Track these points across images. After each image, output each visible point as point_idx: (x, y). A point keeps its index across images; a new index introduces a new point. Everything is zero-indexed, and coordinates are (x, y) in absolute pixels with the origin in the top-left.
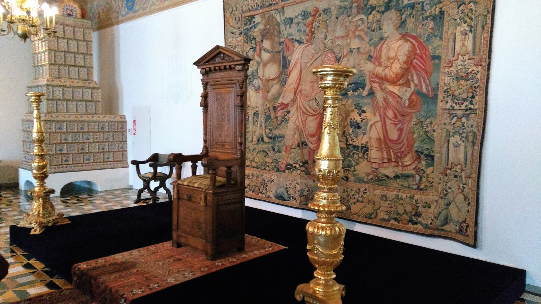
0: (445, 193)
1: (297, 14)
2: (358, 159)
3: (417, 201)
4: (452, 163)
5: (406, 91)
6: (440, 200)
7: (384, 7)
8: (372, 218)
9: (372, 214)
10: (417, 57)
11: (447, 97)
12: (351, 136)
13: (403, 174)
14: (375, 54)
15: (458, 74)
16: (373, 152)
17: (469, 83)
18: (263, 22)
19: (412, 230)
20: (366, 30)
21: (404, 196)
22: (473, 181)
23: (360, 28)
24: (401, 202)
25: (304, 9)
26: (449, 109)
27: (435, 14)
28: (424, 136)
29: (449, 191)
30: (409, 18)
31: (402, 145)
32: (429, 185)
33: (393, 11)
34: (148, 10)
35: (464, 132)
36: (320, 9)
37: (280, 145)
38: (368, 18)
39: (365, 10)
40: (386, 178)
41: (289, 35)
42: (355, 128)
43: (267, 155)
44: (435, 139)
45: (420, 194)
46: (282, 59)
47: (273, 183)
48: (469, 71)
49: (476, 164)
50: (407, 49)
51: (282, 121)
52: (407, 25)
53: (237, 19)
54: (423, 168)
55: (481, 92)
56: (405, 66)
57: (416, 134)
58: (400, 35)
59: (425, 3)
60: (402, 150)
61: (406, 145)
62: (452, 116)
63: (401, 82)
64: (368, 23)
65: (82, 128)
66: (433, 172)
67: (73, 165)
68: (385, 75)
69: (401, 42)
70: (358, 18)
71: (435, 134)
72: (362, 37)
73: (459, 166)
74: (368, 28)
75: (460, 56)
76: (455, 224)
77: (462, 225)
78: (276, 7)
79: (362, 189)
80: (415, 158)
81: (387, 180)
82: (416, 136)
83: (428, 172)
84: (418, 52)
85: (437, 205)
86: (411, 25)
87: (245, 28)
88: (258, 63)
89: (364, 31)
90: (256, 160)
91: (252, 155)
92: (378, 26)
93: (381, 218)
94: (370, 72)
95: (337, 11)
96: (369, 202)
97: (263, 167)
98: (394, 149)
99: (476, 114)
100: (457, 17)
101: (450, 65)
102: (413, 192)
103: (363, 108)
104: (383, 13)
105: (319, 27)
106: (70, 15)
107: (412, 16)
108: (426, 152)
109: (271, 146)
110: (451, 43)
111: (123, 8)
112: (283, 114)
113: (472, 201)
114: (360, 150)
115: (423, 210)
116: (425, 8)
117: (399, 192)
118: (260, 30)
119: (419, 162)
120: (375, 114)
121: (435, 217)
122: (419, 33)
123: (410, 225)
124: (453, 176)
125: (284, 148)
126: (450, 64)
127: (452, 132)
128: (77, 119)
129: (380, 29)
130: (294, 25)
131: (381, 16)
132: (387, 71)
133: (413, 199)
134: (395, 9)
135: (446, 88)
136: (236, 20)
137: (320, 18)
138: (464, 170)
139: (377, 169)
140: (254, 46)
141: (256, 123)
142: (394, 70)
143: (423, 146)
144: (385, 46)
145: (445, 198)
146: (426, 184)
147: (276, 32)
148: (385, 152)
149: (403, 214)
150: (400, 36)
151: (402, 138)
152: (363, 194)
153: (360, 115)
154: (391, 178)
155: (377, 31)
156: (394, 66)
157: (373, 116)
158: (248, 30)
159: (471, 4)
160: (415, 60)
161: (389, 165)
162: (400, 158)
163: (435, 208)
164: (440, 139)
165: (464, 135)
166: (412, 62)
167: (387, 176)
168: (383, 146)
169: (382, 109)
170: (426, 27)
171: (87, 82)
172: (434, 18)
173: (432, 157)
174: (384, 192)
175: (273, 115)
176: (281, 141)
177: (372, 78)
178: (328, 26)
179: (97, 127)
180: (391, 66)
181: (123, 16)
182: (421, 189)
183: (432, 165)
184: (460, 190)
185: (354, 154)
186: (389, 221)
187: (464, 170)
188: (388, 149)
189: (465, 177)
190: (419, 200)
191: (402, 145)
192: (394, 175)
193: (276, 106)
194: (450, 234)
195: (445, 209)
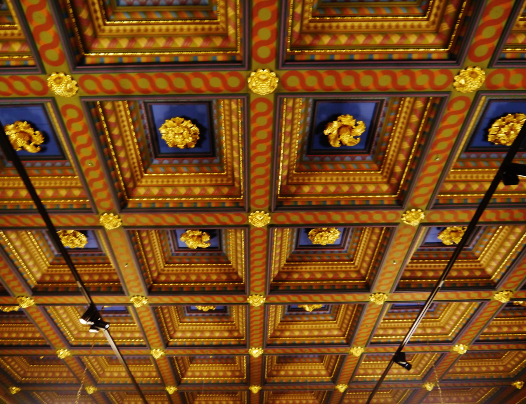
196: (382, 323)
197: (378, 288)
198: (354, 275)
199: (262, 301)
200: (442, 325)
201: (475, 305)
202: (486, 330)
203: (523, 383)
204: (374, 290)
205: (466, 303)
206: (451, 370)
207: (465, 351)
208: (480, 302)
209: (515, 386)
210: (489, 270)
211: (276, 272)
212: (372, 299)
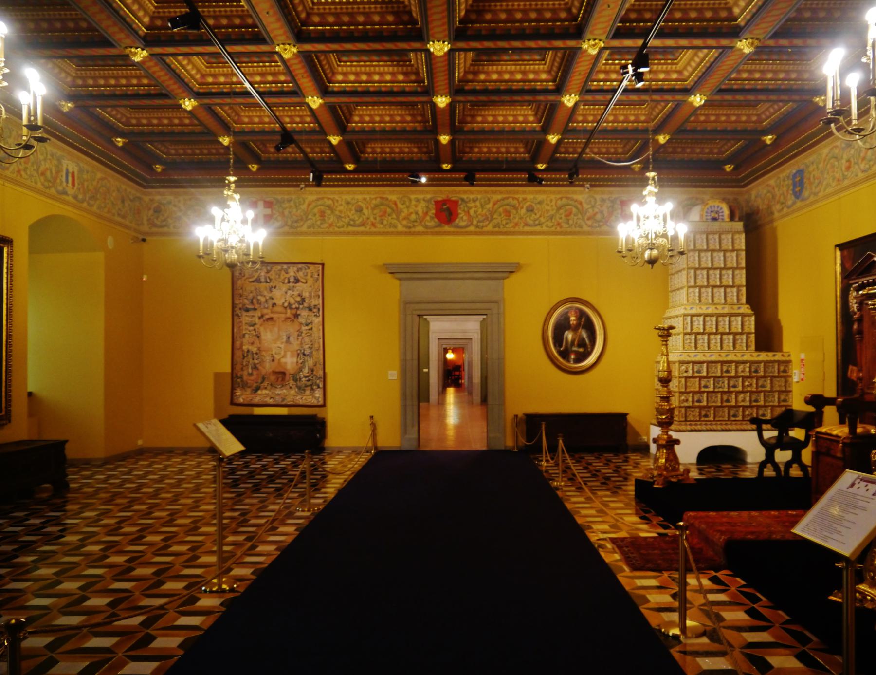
34: (821, 194)
65: (727, 371)
67: (714, 423)
106: (714, 219)
111: (789, 196)
128: (721, 359)
171: (736, 307)
179: (748, 369)
181: (789, 207)
196: (604, 64)
197: (592, 33)
198: (563, 15)
199: (446, 47)
200: (678, 68)
201: (714, 53)
202: (733, 76)
203: (775, 137)
204: (588, 35)
205: (706, 51)
206: (692, 118)
207: (703, 102)
208: (721, 50)
209: (764, 141)
210: (736, 11)
211: (463, 13)
212: (585, 46)
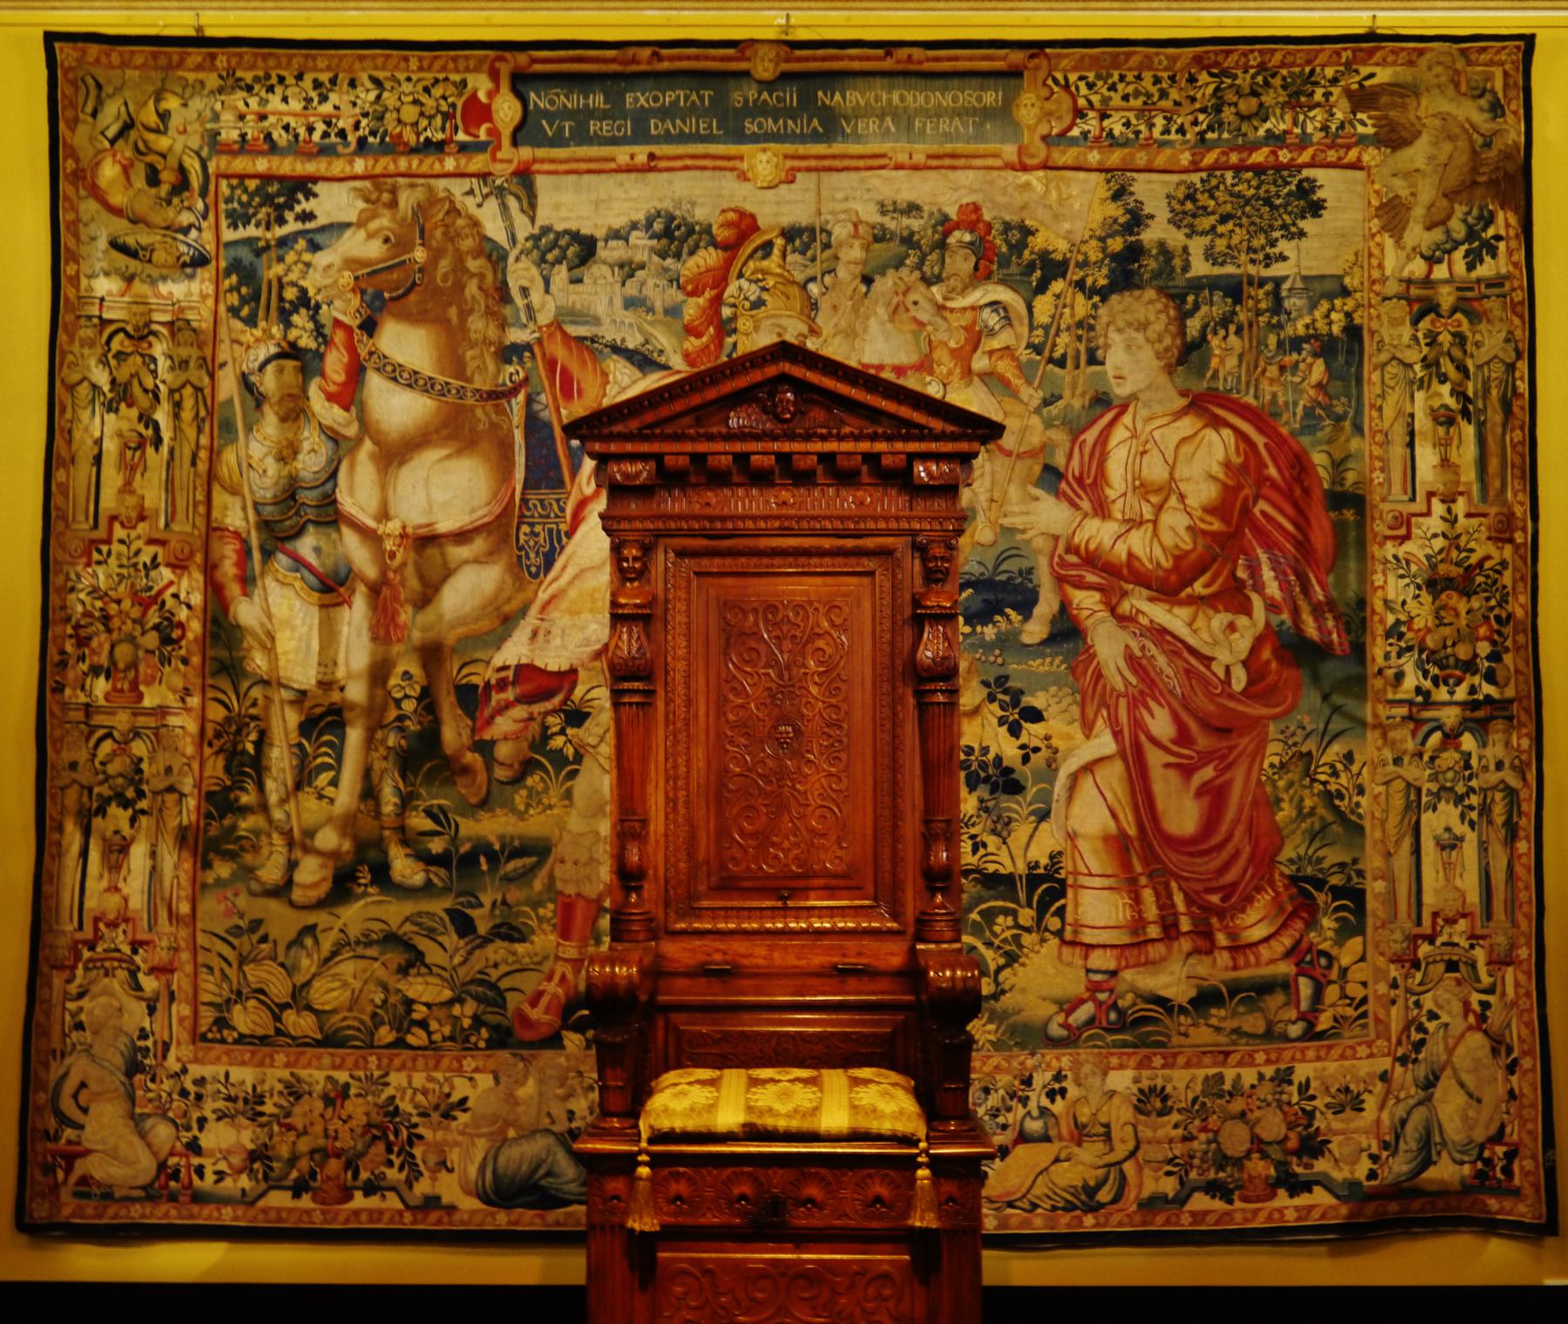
0: (1416, 1036)
1: (619, 222)
2: (1016, 938)
3: (1304, 1088)
4: (1435, 915)
5: (1232, 627)
6: (1399, 1069)
7: (1105, 271)
8: (1102, 1206)
9: (1100, 1185)
10: (1266, 491)
11: (1399, 656)
12: (973, 831)
13: (1235, 980)
14: (1075, 463)
15: (1433, 567)
16: (1087, 897)
17: (1476, 603)
18: (374, 225)
19: (1290, 1217)
20: (1025, 355)
21: (1249, 1076)
22: (1522, 978)
23: (996, 344)
24: (1238, 1105)
25: (667, 205)
26: (1411, 703)
27: (1330, 334)
28: (1321, 811)
29: (1431, 1026)
30: (1222, 333)
31: (1225, 855)
32: (1350, 1012)
33: (1150, 294)
35: (1472, 790)
36: (762, 222)
37: (515, 894)
38: (1030, 308)
39: (1014, 269)
40: (1156, 1011)
41: (566, 315)
42: (992, 792)
43: (414, 961)
44: (1367, 824)
45: (1319, 1059)
46: (519, 436)
47: (463, 1118)
48: (1474, 559)
49: (1526, 908)
50: (1220, 455)
51: (528, 766)
52: (1214, 362)
53: (167, 177)
54: (1325, 946)
55: (1521, 639)
56: (1216, 525)
57: (1285, 805)
58: (1183, 394)
59: (1286, 286)
60: (1231, 876)
61: (1247, 850)
62: (1426, 728)
63: (1198, 587)
64: (1032, 328)
66: (1363, 959)
68: (1130, 555)
69: (1187, 425)
70: (977, 296)
71: (1364, 801)
72: (1006, 383)
73: (1462, 925)
74: (1038, 349)
75: (1435, 502)
76: (1458, 1156)
77: (1487, 1154)
78: (478, 163)
79: (1040, 1079)
80: (1290, 908)
81: (1168, 1021)
82: (1285, 813)
83: (1345, 960)
84: (1272, 471)
85: (1388, 1093)
86: (1232, 362)
87: (229, 235)
88: (334, 437)
89: (1015, 359)
90: (326, 994)
91: (289, 969)
92: (1082, 347)
93: (1145, 1194)
94: (1056, 538)
95: (867, 248)
96: (1081, 1134)
97: (385, 1034)
98: (1186, 879)
99: (1510, 719)
100: (1413, 356)
101: (1402, 531)
102: (1287, 1055)
103: (1027, 700)
104: (1104, 294)
105: (759, 304)
107: (1232, 328)
108: (1335, 880)
109: (438, 906)
110: (1398, 451)
112: (535, 727)
113: (1524, 1053)
114: (1022, 896)
115: (1337, 1124)
116: (1287, 304)
117: (1224, 1064)
118: (351, 263)
119: (1311, 923)
120: (1088, 728)
121: (1385, 1145)
122: (1268, 397)
123: (1282, 1199)
124: (1441, 967)
125: (548, 910)
126: (1403, 528)
127: (1429, 792)
129: (1093, 360)
130: (598, 272)
131: (1095, 307)
132: (1137, 542)
133: (1290, 1083)
134: (1160, 290)
135: (1391, 619)
136: (153, 178)
137: (765, 263)
138: (1483, 937)
139: (1113, 974)
140: (306, 342)
141: (324, 778)
142: (1168, 539)
143: (1320, 853)
144: (1120, 433)
145: (1416, 1061)
146: (1340, 1010)
147: (472, 288)
148: (1148, 895)
149: (1248, 1155)
150: (1184, 402)
151: (1224, 828)
152: (1045, 1102)
153: (1015, 731)
154: (1182, 1009)
155: (1077, 367)
156: (1167, 519)
157: (1080, 736)
158: (258, 253)
159: (1458, 316)
160: (1262, 505)
161: (1169, 949)
162: (1221, 914)
163: (1382, 1107)
164: (1383, 822)
165: (1474, 800)
166: (1246, 511)
167: (1162, 1002)
168: (1138, 868)
169: (1123, 703)
170: (1297, 379)
172: (1326, 348)
173: (1358, 896)
174: (1156, 1076)
175: (453, 733)
176: (526, 875)
177: (1063, 564)
178: (814, 306)
180: (1155, 522)
182: (1321, 1036)
183: (1360, 930)
184: (1471, 1019)
185: (990, 916)
186: (1181, 1200)
187: (1483, 937)
188: (1161, 877)
189: (1489, 963)
190: (1314, 1084)
191: (1225, 855)
192: (1193, 993)
193: (475, 680)
194: (1441, 1204)
195: (1420, 1103)
